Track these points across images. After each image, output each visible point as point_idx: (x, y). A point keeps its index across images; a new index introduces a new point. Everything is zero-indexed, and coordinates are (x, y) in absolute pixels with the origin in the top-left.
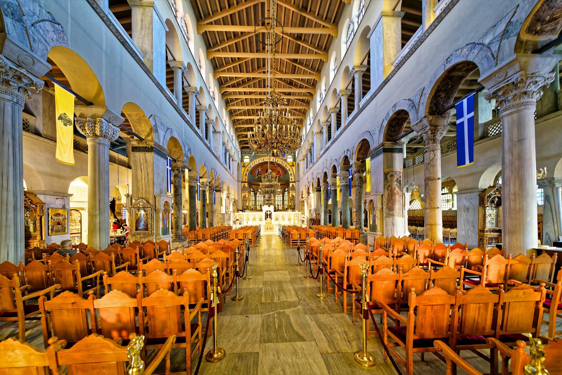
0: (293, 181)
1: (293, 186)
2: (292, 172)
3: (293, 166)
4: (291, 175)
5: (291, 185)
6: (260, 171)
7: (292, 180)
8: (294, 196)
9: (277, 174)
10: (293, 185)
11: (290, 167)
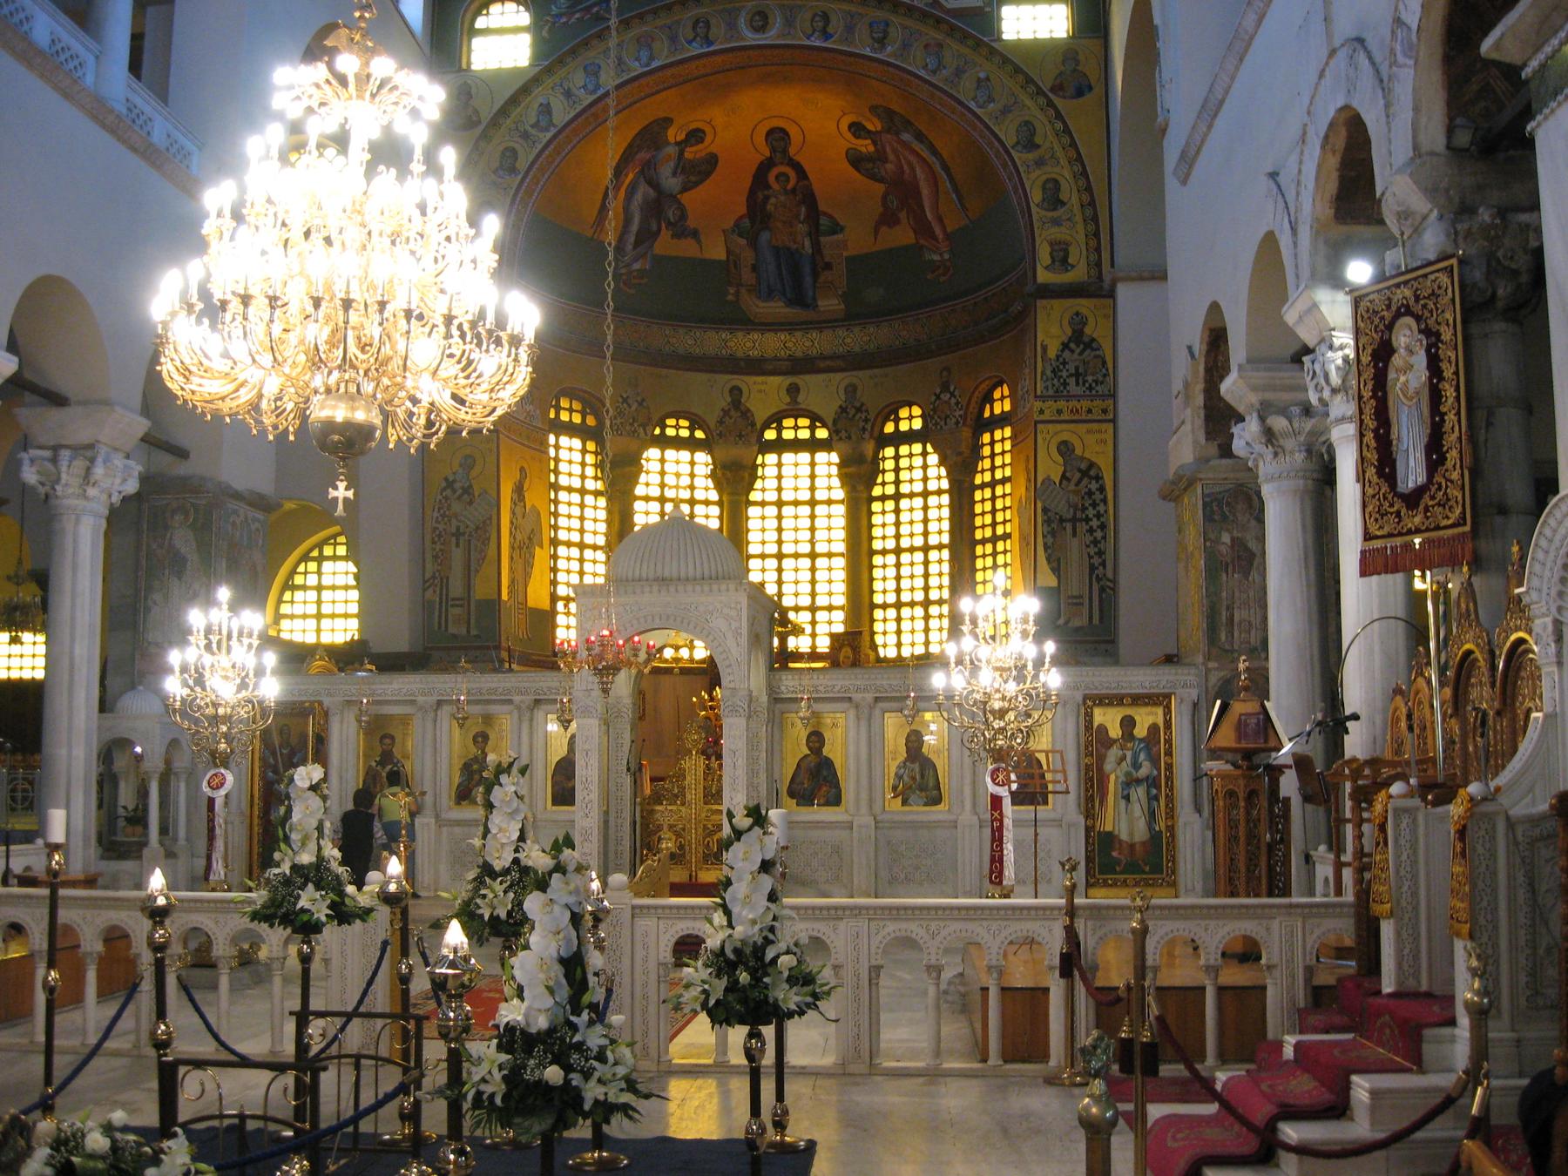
0: (1078, 273)
1: (1078, 338)
2: (1065, 174)
3: (1080, 93)
4: (1054, 199)
5: (1050, 327)
6: (671, 183)
7: (1061, 259)
8: (1090, 471)
9: (888, 219)
10: (1078, 323)
11: (1032, 109)
